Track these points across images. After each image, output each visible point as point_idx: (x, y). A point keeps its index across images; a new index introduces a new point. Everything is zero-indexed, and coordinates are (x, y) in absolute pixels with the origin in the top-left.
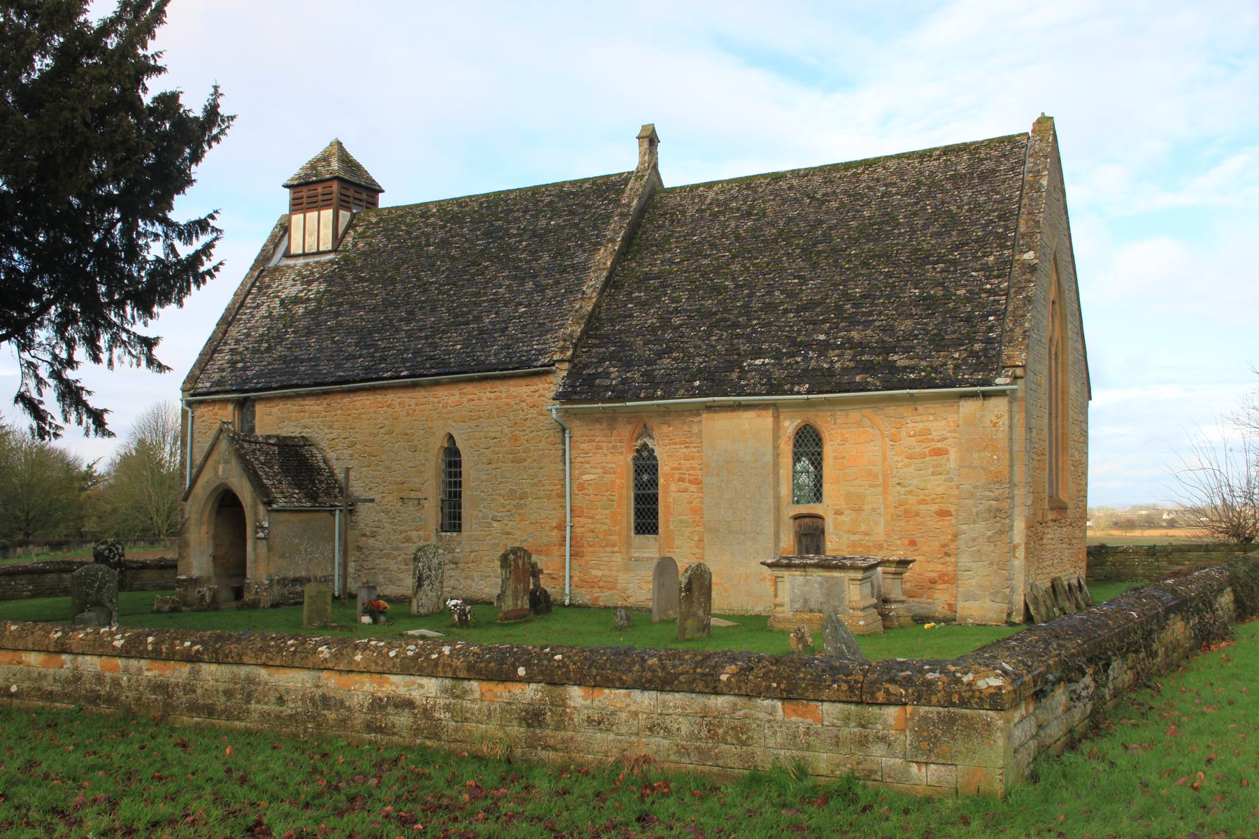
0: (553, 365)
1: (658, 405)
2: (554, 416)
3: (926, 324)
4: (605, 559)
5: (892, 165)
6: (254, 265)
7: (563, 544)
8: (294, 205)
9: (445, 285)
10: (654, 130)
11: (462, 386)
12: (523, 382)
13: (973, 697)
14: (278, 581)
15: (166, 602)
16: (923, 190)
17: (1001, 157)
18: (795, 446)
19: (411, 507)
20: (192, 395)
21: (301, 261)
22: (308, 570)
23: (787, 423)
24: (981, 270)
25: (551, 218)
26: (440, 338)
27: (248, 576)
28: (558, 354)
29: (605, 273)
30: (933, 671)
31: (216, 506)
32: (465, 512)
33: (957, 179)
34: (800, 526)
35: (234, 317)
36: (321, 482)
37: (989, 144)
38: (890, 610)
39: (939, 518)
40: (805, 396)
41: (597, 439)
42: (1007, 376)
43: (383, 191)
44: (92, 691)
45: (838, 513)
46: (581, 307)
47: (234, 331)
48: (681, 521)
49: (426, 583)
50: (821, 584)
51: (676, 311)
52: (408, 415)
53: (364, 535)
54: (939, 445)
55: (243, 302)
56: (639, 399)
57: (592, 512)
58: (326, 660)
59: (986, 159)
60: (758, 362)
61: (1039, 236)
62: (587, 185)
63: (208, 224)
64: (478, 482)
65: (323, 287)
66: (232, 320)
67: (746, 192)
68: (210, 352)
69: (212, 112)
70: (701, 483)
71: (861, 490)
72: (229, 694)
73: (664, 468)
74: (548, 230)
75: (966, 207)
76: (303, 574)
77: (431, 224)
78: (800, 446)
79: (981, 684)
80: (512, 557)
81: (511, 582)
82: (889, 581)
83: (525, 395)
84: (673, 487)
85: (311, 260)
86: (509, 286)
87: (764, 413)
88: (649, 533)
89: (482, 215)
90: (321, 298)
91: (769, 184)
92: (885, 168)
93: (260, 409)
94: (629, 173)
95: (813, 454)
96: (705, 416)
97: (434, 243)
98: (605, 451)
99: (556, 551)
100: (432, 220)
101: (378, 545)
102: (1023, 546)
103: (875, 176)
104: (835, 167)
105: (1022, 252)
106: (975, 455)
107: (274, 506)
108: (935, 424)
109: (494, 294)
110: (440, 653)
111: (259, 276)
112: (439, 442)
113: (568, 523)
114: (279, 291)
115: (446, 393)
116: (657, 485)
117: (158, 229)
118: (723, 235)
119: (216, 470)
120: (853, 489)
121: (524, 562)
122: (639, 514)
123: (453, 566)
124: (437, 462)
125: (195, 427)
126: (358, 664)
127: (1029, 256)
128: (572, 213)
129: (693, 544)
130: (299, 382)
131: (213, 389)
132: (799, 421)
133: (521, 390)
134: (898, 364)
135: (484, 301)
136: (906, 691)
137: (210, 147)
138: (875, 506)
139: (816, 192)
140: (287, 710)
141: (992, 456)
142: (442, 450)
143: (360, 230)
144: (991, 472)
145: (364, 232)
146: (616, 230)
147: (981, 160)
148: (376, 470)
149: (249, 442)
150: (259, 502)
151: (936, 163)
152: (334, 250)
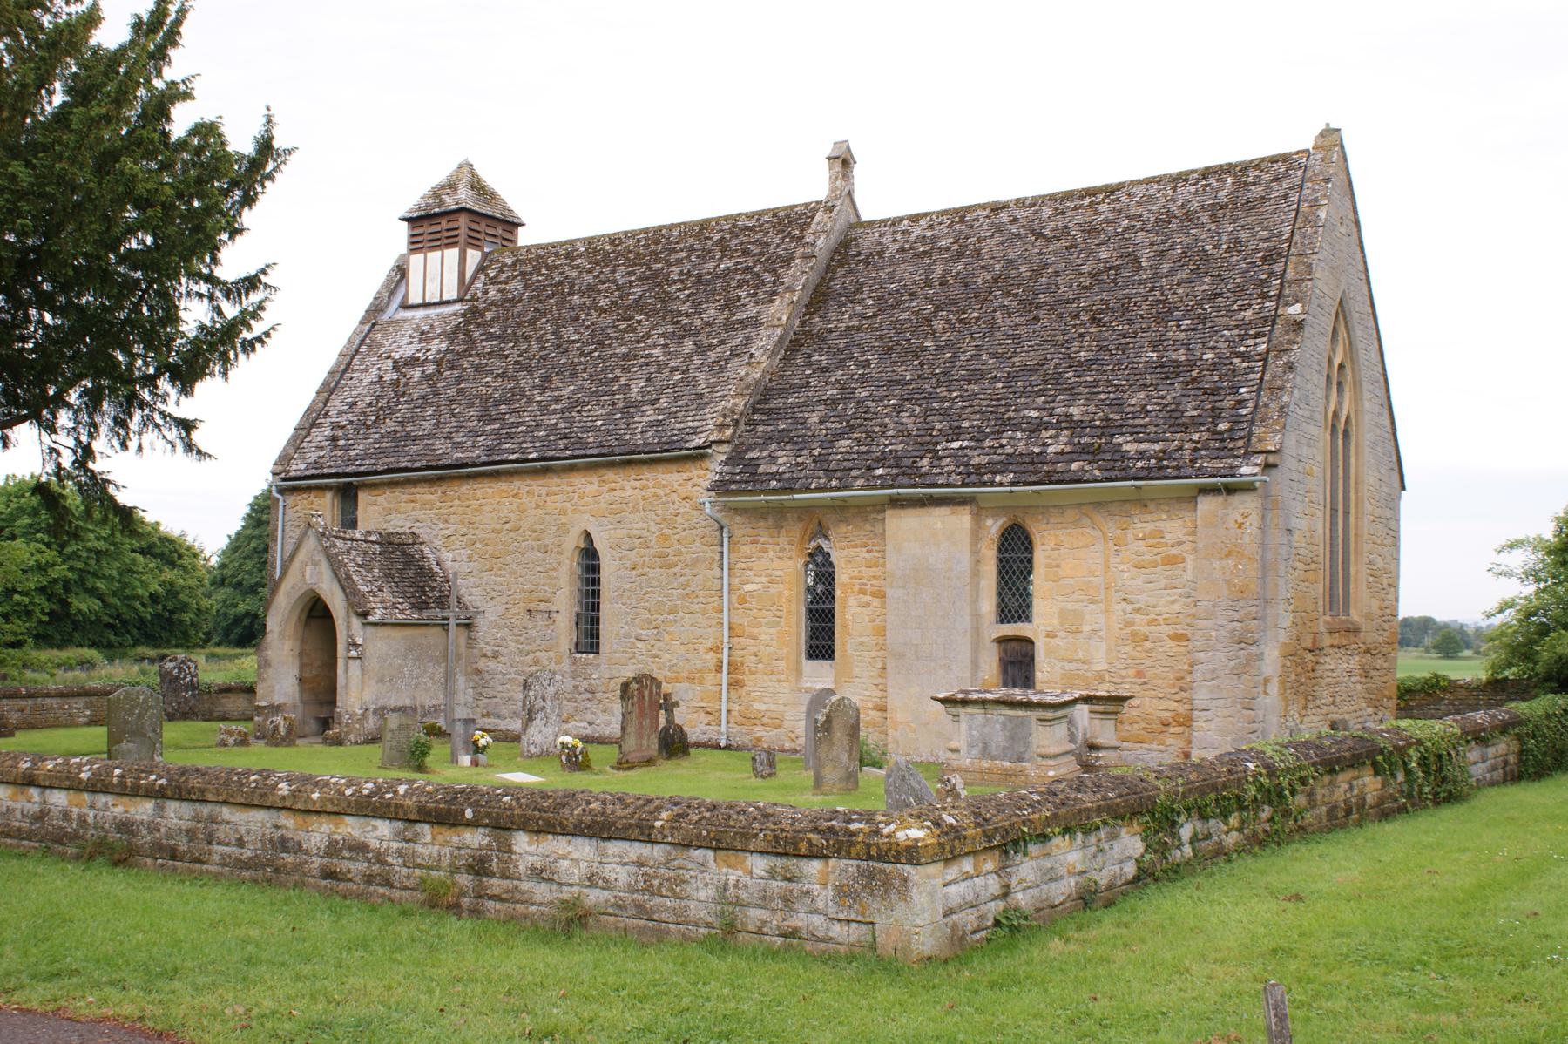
0: (709, 447)
1: (832, 498)
2: (708, 511)
3: (1164, 398)
4: (771, 689)
5: (1139, 191)
6: (364, 318)
7: (719, 669)
8: (413, 243)
9: (588, 344)
10: (848, 148)
11: (602, 471)
12: (674, 467)
13: (890, 850)
14: (375, 711)
15: (230, 733)
16: (1174, 224)
17: (1272, 181)
18: (999, 550)
19: (540, 620)
20: (284, 479)
21: (420, 313)
22: (414, 698)
23: (989, 522)
24: (1237, 327)
25: (721, 260)
26: (579, 412)
27: (339, 704)
28: (716, 433)
29: (779, 331)
30: (860, 821)
31: (304, 617)
32: (605, 628)
33: (1215, 209)
34: (1005, 651)
35: (338, 383)
36: (433, 589)
37: (1257, 165)
38: (1098, 757)
39: (1174, 644)
40: (1008, 489)
41: (762, 540)
42: (1256, 465)
43: (523, 225)
44: (61, 828)
46: (747, 375)
47: (337, 404)
48: (862, 644)
49: (539, 716)
50: (1004, 724)
51: (863, 381)
52: (538, 506)
53: (485, 655)
54: (1174, 551)
55: (349, 364)
56: (808, 490)
57: (756, 630)
58: (284, 798)
59: (1254, 184)
60: (955, 445)
61: (1309, 283)
62: (766, 218)
63: (260, 281)
64: (620, 592)
65: (444, 346)
66: (336, 386)
67: (958, 227)
68: (307, 425)
69: (265, 147)
70: (884, 596)
71: (1077, 606)
72: (191, 834)
73: (841, 578)
74: (715, 276)
75: (1225, 247)
76: (408, 702)
77: (578, 267)
78: (1006, 550)
79: (901, 835)
80: (635, 686)
81: (634, 716)
82: (1097, 722)
84: (852, 601)
85: (433, 312)
86: (666, 346)
87: (960, 509)
88: (824, 658)
89: (637, 254)
90: (442, 359)
91: (988, 217)
92: (1129, 195)
93: (363, 497)
94: (817, 203)
95: (1022, 561)
96: (888, 512)
97: (579, 291)
98: (771, 555)
99: (710, 678)
100: (578, 262)
101: (501, 668)
102: (1276, 679)
103: (1117, 206)
104: (1069, 195)
105: (1287, 305)
106: (1216, 564)
107: (371, 619)
108: (1168, 524)
109: (647, 356)
110: (396, 792)
111: (369, 331)
112: (573, 541)
113: (725, 645)
114: (392, 351)
115: (583, 480)
116: (833, 598)
117: (203, 288)
118: (928, 284)
119: (303, 574)
120: (1070, 606)
121: (651, 692)
123: (589, 696)
124: (571, 566)
125: (287, 518)
126: (314, 802)
127: (1295, 309)
128: (746, 253)
129: (875, 672)
130: (409, 465)
131: (308, 473)
132: (1004, 519)
133: (672, 478)
134: (1125, 447)
135: (634, 365)
136: (827, 841)
137: (264, 187)
138: (1095, 627)
139: (1043, 228)
140: (247, 853)
141: (1236, 565)
142: (577, 552)
143: (492, 273)
144: (1235, 585)
145: (497, 276)
146: (799, 277)
147: (1247, 184)
148: (500, 576)
149: (344, 539)
150: (352, 614)
151: (1192, 189)
152: (460, 300)
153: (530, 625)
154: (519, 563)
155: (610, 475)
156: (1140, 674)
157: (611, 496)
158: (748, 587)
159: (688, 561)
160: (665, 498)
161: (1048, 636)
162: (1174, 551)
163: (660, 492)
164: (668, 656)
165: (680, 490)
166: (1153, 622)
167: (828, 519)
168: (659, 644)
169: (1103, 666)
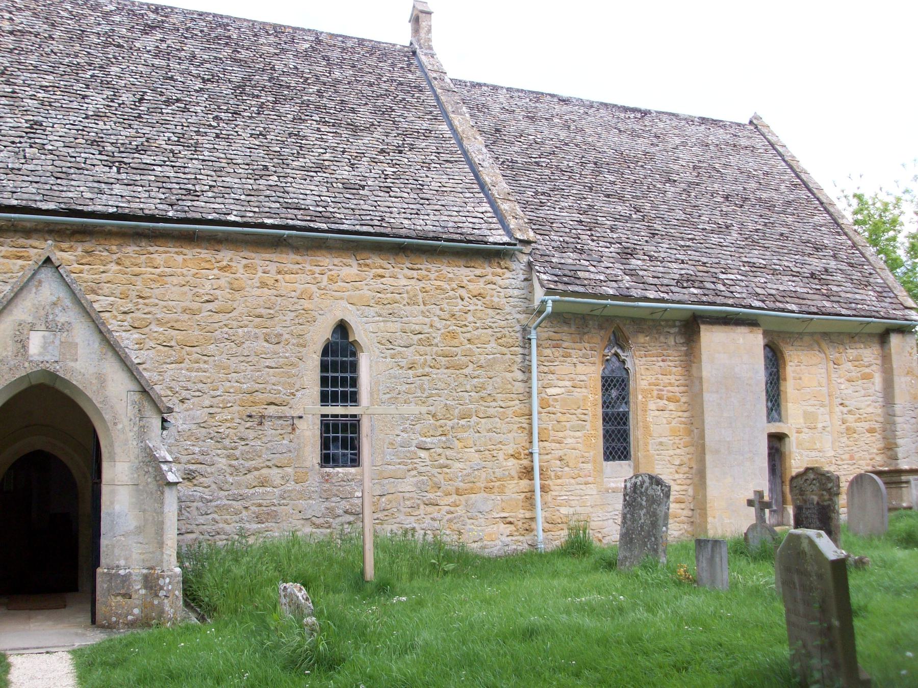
39: (869, 435)
45: (799, 432)
48: (661, 444)
54: (867, 370)
57: (561, 434)
83: (465, 280)
84: (652, 406)
88: (620, 459)
112: (322, 333)
119: (23, 345)
122: (608, 436)
138: (824, 424)
153: (251, 434)
154: (232, 355)
155: (376, 260)
156: (852, 458)
157: (377, 284)
158: (551, 391)
159: (483, 362)
160: (451, 293)
161: (797, 432)
162: (867, 370)
163: (445, 285)
164: (461, 465)
165: (471, 286)
166: (858, 420)
167: (627, 329)
168: (448, 452)
169: (832, 453)
